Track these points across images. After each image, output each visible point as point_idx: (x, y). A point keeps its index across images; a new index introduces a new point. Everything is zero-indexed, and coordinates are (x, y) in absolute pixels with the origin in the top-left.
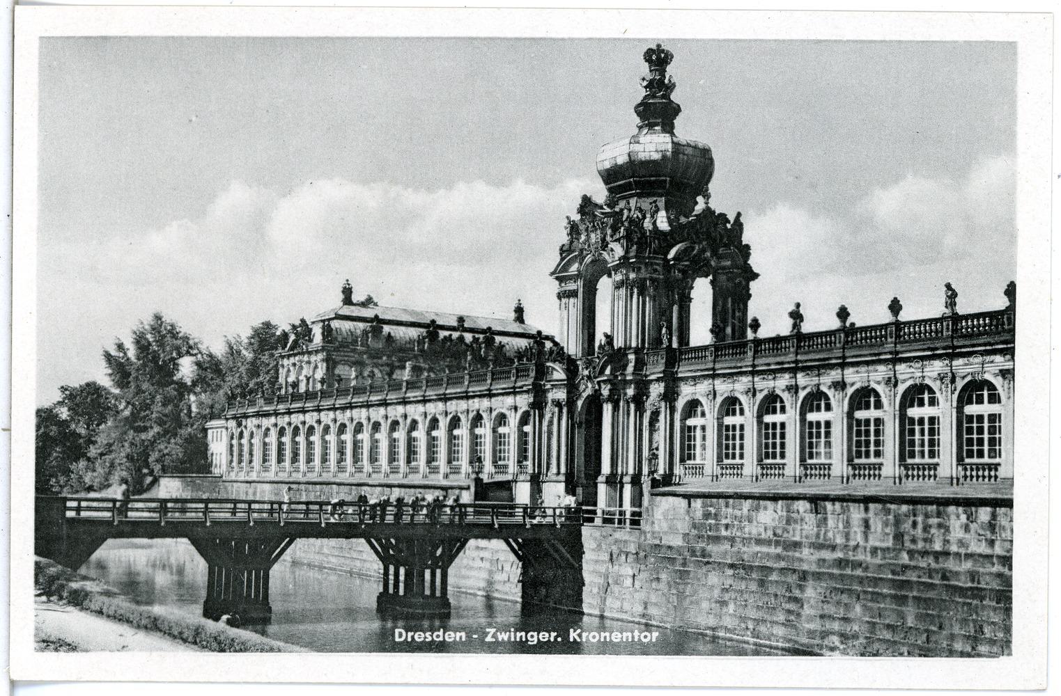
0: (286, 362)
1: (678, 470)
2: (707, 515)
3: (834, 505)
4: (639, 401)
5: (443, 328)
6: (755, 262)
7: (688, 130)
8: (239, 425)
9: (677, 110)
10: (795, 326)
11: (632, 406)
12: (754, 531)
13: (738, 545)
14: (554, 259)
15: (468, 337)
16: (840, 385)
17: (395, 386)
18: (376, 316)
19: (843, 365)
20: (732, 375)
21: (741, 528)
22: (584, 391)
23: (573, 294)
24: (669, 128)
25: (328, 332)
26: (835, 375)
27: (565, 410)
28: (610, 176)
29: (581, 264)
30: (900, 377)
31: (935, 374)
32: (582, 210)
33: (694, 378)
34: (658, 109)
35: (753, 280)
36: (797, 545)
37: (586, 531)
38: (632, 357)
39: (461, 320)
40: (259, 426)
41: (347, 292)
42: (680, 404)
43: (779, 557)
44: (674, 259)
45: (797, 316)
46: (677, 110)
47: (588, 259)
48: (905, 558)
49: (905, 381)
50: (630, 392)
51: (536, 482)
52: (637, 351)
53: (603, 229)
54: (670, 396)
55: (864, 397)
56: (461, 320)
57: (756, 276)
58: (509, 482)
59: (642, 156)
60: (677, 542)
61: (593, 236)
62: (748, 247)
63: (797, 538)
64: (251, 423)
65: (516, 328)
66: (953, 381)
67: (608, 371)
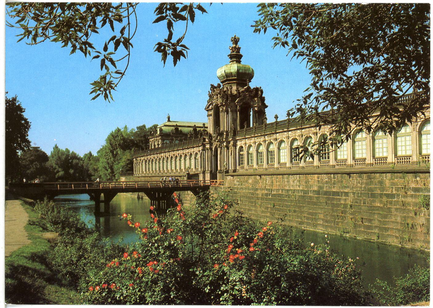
0: (151, 140)
4: (228, 148)
5: (198, 127)
6: (266, 102)
7: (244, 61)
8: (136, 160)
9: (241, 56)
16: (276, 139)
17: (175, 145)
18: (177, 125)
19: (276, 133)
20: (250, 138)
21: (245, 185)
23: (211, 115)
24: (239, 62)
25: (161, 130)
26: (274, 136)
33: (241, 139)
34: (236, 56)
38: (225, 133)
40: (140, 160)
41: (169, 118)
42: (238, 147)
44: (237, 102)
46: (241, 56)
47: (214, 104)
49: (291, 137)
52: (227, 132)
54: (235, 145)
56: (204, 124)
57: (267, 107)
58: (198, 174)
62: (264, 98)
64: (139, 159)
66: (302, 137)
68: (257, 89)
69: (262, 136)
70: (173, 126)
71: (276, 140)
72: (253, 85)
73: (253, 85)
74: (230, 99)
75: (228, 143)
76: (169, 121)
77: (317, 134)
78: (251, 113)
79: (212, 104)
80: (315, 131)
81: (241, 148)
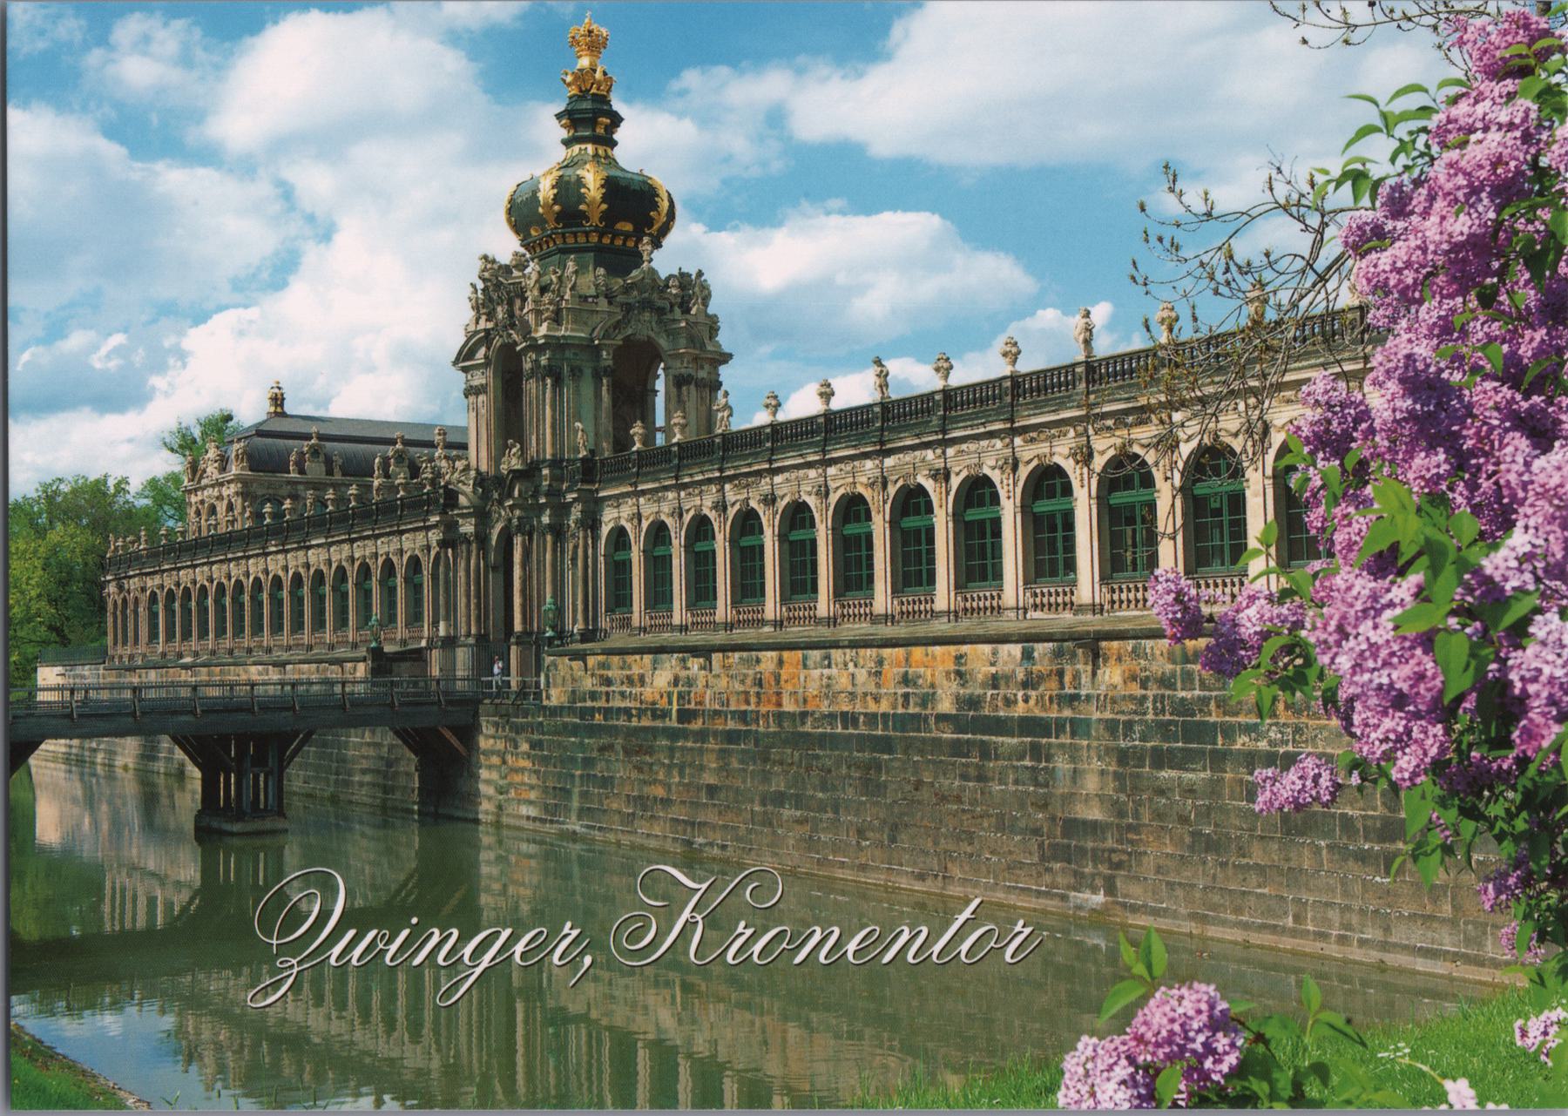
1: (604, 622)
4: (558, 531)
6: (725, 340)
11: (549, 538)
20: (656, 490)
26: (764, 485)
29: (488, 349)
30: (832, 485)
31: (864, 480)
35: (726, 362)
38: (545, 472)
42: (605, 530)
47: (497, 342)
50: (546, 520)
52: (556, 463)
53: (511, 303)
54: (591, 523)
58: (420, 651)
61: (499, 309)
63: (692, 706)
66: (885, 486)
67: (516, 493)
68: (684, 280)
69: (709, 481)
71: (774, 501)
72: (665, 261)
73: (665, 261)
75: (562, 510)
77: (947, 478)
78: (660, 385)
79: (487, 337)
80: (939, 464)
81: (619, 537)
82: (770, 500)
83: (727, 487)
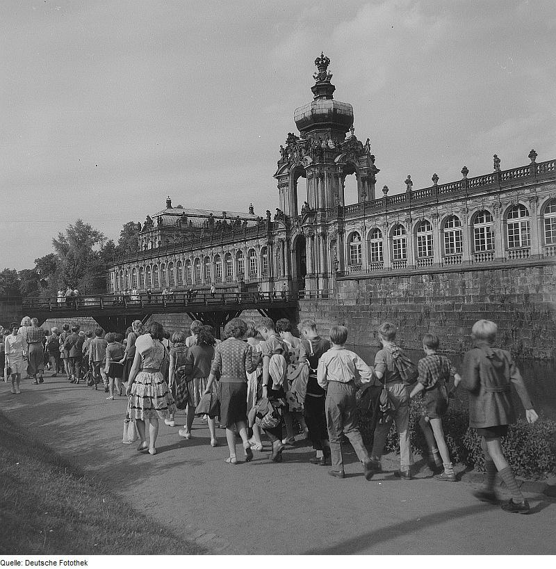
2: (369, 288)
3: (443, 276)
4: (324, 235)
8: (120, 268)
10: (408, 187)
11: (321, 238)
12: (397, 294)
13: (388, 303)
14: (275, 169)
15: (229, 221)
16: (436, 216)
20: (375, 216)
22: (291, 234)
23: (287, 185)
25: (160, 220)
26: (433, 210)
27: (286, 243)
28: (300, 124)
32: (288, 142)
36: (423, 299)
37: (301, 303)
39: (224, 213)
41: (169, 202)
42: (347, 235)
43: (412, 307)
45: (409, 182)
47: (293, 167)
48: (488, 301)
51: (272, 280)
52: (323, 210)
53: (300, 151)
54: (341, 232)
55: (450, 220)
59: (318, 112)
60: (353, 304)
64: (126, 266)
65: (250, 216)
70: (178, 215)
74: (326, 156)
76: (169, 206)
82: (437, 215)
83: (412, 212)
